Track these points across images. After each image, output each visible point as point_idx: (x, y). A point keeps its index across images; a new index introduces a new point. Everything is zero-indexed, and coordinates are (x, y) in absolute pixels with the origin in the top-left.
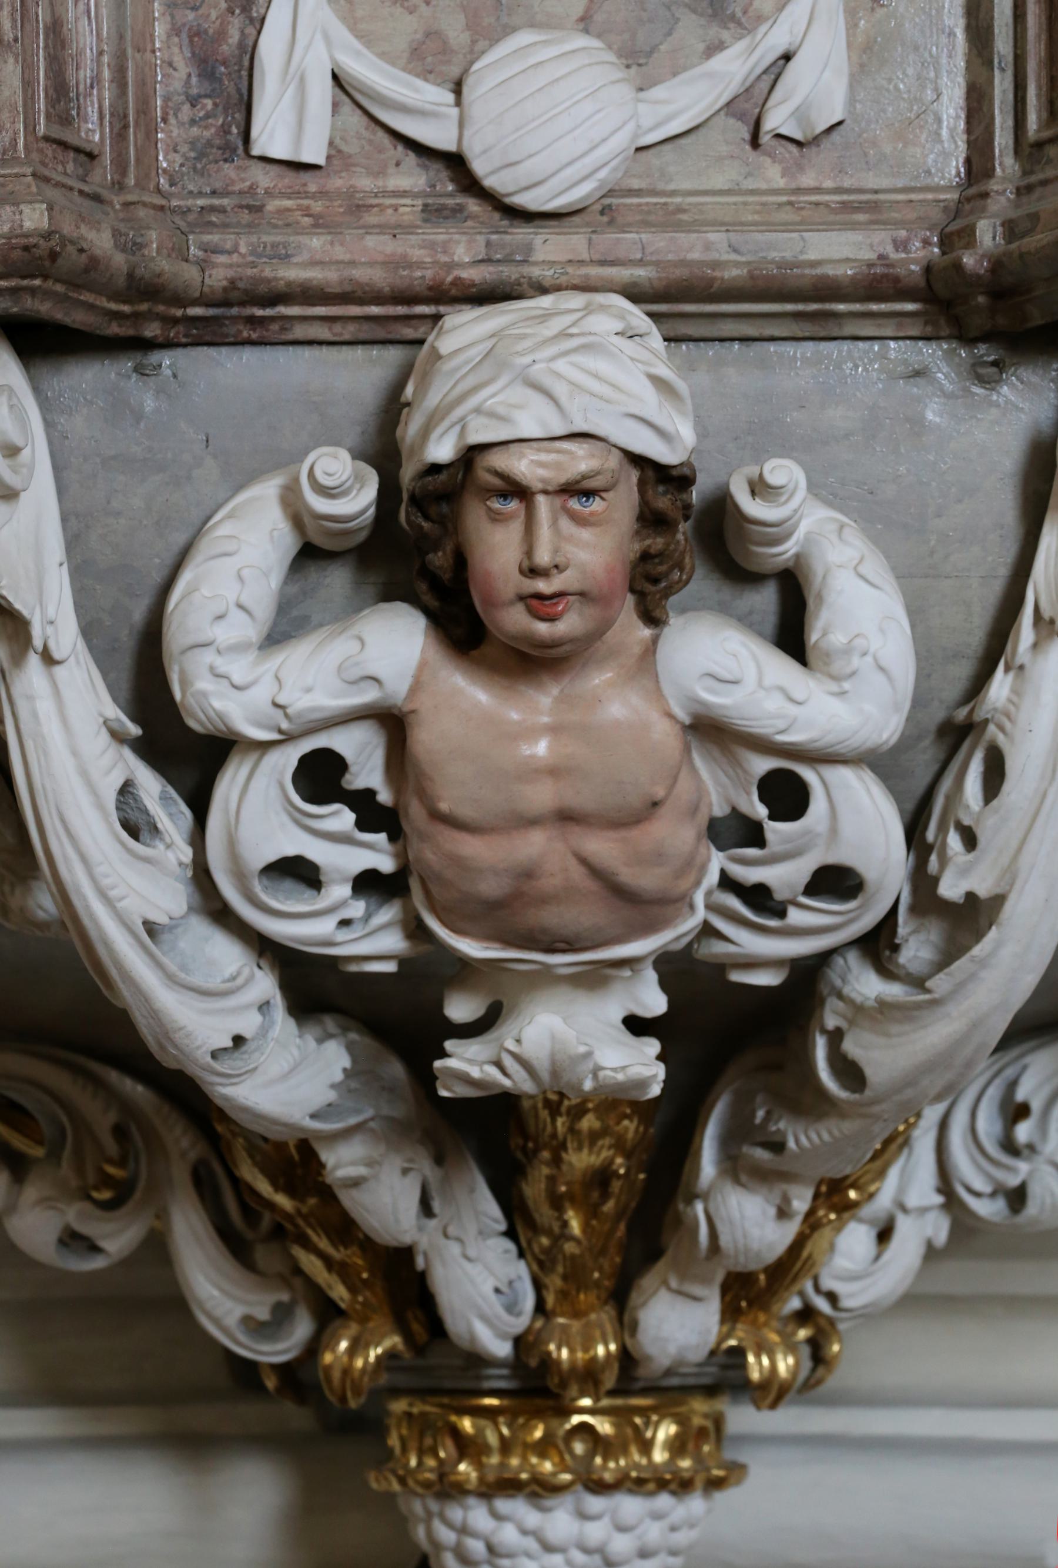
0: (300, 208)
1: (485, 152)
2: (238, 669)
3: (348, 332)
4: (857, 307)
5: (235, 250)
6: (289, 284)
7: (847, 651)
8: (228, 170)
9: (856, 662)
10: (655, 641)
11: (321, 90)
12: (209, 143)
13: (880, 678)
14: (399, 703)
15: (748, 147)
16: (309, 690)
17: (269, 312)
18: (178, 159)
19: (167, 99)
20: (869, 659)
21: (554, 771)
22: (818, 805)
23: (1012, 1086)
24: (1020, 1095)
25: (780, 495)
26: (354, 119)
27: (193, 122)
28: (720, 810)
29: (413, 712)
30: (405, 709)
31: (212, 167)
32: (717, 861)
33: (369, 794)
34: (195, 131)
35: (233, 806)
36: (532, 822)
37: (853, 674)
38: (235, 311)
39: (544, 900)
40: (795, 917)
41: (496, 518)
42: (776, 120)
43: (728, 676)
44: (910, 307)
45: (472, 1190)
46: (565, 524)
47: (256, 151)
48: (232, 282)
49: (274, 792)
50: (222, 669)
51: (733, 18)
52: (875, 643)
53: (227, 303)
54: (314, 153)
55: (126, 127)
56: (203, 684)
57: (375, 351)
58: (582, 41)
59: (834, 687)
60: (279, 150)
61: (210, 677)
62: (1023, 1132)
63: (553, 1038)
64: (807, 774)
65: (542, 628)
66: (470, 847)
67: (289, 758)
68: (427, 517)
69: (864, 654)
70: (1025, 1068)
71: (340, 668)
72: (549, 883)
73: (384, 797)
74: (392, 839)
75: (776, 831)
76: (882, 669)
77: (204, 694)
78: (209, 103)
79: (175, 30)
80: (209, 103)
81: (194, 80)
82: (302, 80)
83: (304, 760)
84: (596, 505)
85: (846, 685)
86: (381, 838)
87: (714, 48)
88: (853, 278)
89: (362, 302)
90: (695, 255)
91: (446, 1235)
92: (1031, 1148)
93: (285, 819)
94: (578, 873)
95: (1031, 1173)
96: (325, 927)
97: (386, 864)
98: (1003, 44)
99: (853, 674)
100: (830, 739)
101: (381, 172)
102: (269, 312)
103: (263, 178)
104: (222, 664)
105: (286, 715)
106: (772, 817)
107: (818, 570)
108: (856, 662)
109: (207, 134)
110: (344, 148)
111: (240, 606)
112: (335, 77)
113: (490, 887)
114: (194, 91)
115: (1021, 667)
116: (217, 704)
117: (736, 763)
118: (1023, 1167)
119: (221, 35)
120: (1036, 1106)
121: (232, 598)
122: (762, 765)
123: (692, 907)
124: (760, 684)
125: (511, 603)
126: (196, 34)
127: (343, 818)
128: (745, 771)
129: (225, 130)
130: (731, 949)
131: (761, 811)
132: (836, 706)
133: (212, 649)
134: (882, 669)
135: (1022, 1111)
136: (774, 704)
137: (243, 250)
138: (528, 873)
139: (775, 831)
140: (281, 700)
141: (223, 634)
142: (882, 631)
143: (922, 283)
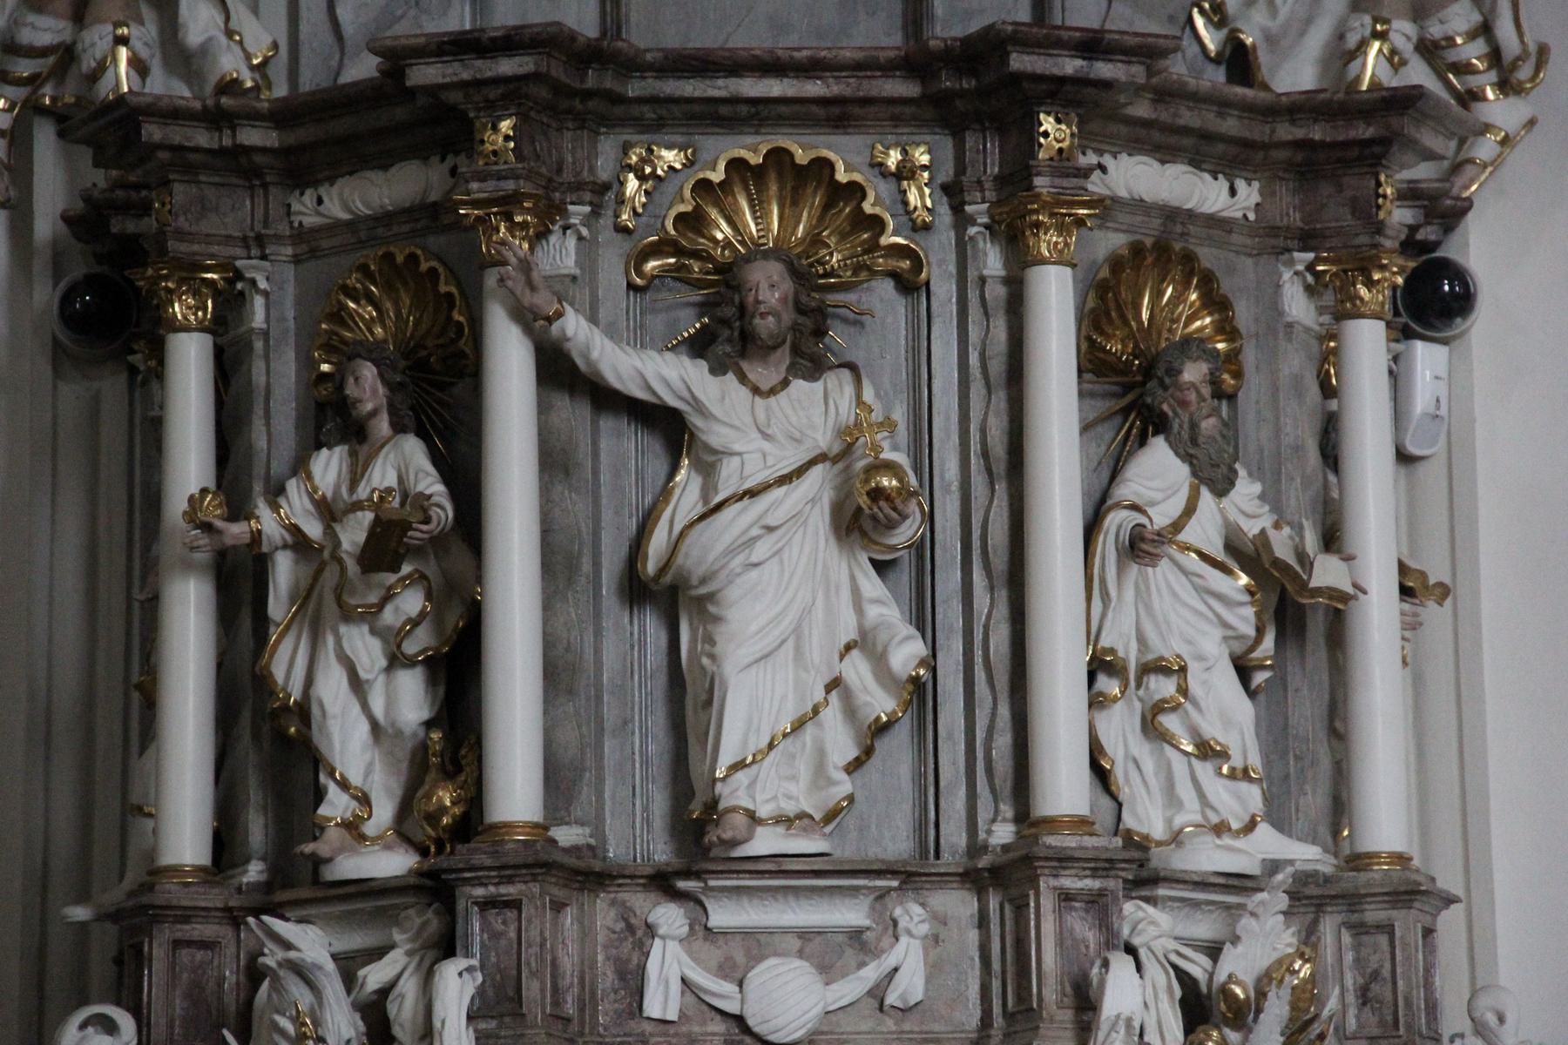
42: (892, 999)
54: (672, 1015)
58: (797, 963)
87: (862, 965)
98: (996, 966)
103: (648, 1028)
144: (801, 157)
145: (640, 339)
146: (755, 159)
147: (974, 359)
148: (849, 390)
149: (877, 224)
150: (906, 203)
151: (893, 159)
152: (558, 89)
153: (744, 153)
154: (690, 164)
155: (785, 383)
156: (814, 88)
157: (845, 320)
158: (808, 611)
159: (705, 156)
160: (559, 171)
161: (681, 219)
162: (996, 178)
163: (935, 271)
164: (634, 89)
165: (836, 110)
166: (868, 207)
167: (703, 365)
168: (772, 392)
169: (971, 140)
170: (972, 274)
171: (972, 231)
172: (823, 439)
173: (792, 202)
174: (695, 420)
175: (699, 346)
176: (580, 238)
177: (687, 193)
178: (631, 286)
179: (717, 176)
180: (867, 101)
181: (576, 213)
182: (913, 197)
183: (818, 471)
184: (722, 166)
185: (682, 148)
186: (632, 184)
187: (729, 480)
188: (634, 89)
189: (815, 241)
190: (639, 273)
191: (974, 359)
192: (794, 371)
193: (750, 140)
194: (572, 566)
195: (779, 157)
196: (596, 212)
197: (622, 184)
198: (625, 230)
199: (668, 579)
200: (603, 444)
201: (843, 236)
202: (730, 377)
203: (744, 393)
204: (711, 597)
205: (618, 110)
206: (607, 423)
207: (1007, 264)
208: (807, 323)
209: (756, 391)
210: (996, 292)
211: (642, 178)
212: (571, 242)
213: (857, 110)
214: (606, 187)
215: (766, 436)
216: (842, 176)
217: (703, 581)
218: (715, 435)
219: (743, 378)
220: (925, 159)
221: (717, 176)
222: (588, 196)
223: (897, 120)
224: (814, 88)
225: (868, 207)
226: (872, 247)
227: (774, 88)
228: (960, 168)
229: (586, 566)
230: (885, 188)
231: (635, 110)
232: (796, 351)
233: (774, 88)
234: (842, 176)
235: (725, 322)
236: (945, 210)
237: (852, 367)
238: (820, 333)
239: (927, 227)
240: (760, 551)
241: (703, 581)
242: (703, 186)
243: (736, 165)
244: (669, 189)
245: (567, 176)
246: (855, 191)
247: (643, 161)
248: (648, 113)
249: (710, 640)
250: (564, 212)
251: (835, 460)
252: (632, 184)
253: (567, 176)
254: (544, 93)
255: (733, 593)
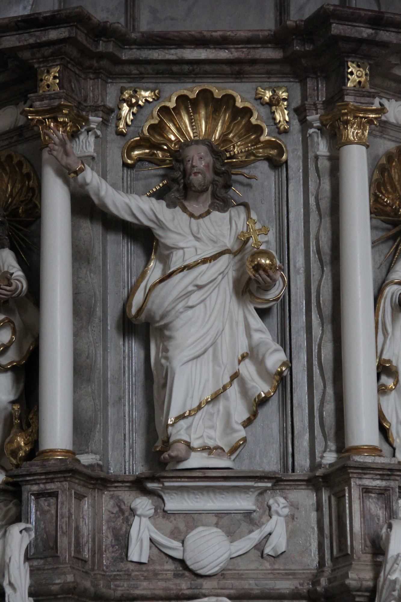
144: (218, 94)
145: (129, 190)
146: (193, 96)
147: (312, 200)
148: (243, 216)
149: (258, 130)
150: (274, 119)
151: (268, 94)
152: (84, 51)
153: (186, 92)
154: (157, 99)
155: (208, 213)
156: (224, 54)
157: (241, 184)
158: (220, 333)
159: (165, 95)
160: (85, 101)
161: (152, 127)
162: (324, 102)
163: (291, 155)
164: (125, 55)
165: (236, 68)
166: (253, 120)
167: (164, 203)
168: (201, 216)
169: (310, 83)
170: (311, 155)
171: (311, 131)
172: (229, 242)
173: (212, 120)
174: (158, 232)
175: (159, 195)
176: (97, 137)
177: (155, 113)
178: (125, 165)
179: (172, 104)
180: (253, 62)
181: (95, 120)
182: (278, 117)
183: (225, 258)
184: (174, 99)
185: (153, 90)
186: (125, 108)
187: (176, 262)
188: (125, 55)
189: (224, 139)
190: (129, 157)
191: (312, 200)
192: (213, 207)
193: (189, 86)
194: (91, 313)
195: (205, 94)
196: (105, 123)
197: (120, 109)
198: (120, 134)
199: (143, 317)
200: (109, 248)
201: (240, 137)
202: (178, 209)
203: (185, 216)
204: (166, 327)
205: (118, 69)
206: (111, 238)
207: (330, 150)
208: (220, 180)
209: (192, 215)
210: (324, 164)
211: (131, 106)
212: (92, 139)
213: (247, 68)
214: (111, 111)
215: (197, 239)
216: (239, 104)
217: (162, 317)
218: (169, 239)
219: (185, 209)
220: (284, 95)
221: (172, 104)
222: (101, 113)
223: (269, 74)
224: (224, 54)
225: (253, 120)
226: (257, 141)
227: (202, 54)
228: (304, 97)
229: (99, 311)
230: (264, 111)
231: (127, 68)
232: (214, 196)
233: (202, 54)
234: (239, 104)
235: (175, 180)
236: (296, 123)
237: (245, 205)
238: (227, 187)
239: (286, 132)
240: (194, 299)
241: (162, 317)
242: (164, 110)
243: (182, 99)
244: (146, 112)
245: (90, 103)
246: (247, 112)
247: (131, 96)
248: (134, 70)
249: (166, 350)
250: (87, 121)
251: (235, 254)
252: (125, 108)
253: (90, 103)
254: (75, 53)
255: (178, 323)
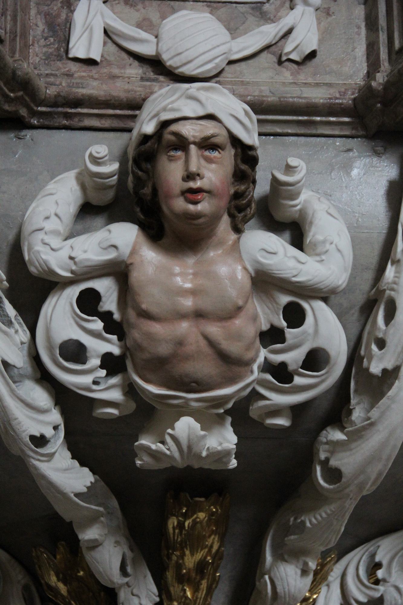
0: (89, 76)
1: (168, 50)
2: (55, 242)
3: (106, 123)
4: (324, 119)
5: (61, 84)
6: (83, 95)
7: (324, 242)
8: (59, 64)
9: (328, 246)
10: (239, 239)
11: (99, 36)
12: (51, 54)
13: (338, 255)
14: (126, 259)
15: (276, 65)
16: (85, 252)
17: (73, 111)
18: (38, 59)
19: (34, 37)
20: (333, 246)
21: (193, 292)
22: (309, 319)
23: (373, 556)
24: (377, 559)
25: (295, 172)
26: (112, 48)
27: (44, 46)
28: (265, 327)
29: (131, 264)
30: (128, 262)
31: (52, 63)
32: (263, 353)
33: (109, 314)
34: (45, 50)
35: (49, 314)
36: (182, 316)
37: (327, 251)
38: (60, 109)
39: (187, 358)
40: (298, 380)
41: (171, 159)
43: (272, 251)
44: (346, 119)
45: (145, 577)
46: (203, 162)
47: (71, 55)
48: (58, 93)
49: (68, 308)
50: (47, 241)
51: (269, 19)
52: (336, 240)
53: (55, 105)
55: (16, 36)
56: (39, 247)
57: (119, 134)
59: (318, 258)
60: (82, 55)
61: (41, 244)
62: (380, 574)
63: (189, 428)
64: (305, 305)
65: (191, 207)
66: (156, 328)
67: (74, 292)
68: (141, 170)
69: (332, 243)
70: (379, 547)
71: (99, 244)
72: (190, 348)
73: (117, 316)
74: (120, 339)
75: (290, 333)
76: (339, 250)
77: (38, 252)
78: (52, 40)
79: (39, 13)
80: (52, 40)
81: (46, 30)
82: (91, 29)
83: (82, 293)
84: (215, 154)
85: (323, 257)
86: (114, 338)
88: (323, 104)
89: (114, 107)
90: (256, 93)
91: (133, 595)
92: (384, 580)
93: (72, 322)
94: (203, 343)
95: (385, 591)
96: (87, 380)
97: (116, 351)
99: (327, 251)
100: (316, 280)
101: (124, 67)
102: (73, 111)
104: (47, 239)
105: (75, 263)
106: (288, 327)
107: (310, 212)
108: (328, 246)
109: (50, 50)
110: (108, 58)
111: (56, 215)
112: (106, 32)
113: (164, 350)
114: (45, 35)
115: (399, 261)
116: (44, 257)
117: (274, 300)
118: (381, 588)
119: (58, 15)
120: (385, 563)
121: (53, 212)
122: (285, 299)
123: (252, 372)
124: (286, 255)
125: (178, 196)
126: (47, 15)
127: (98, 325)
128: (277, 303)
129: (58, 49)
130: (267, 402)
131: (285, 324)
132: (318, 266)
133: (43, 232)
134: (339, 250)
135: (378, 566)
136: (292, 263)
137: (64, 84)
138: (180, 343)
139: (290, 333)
140: (73, 255)
141: (49, 226)
142: (339, 235)
143: (352, 106)
